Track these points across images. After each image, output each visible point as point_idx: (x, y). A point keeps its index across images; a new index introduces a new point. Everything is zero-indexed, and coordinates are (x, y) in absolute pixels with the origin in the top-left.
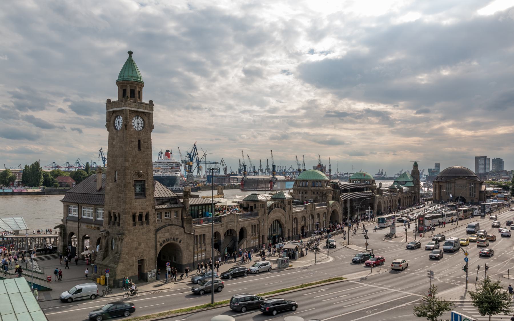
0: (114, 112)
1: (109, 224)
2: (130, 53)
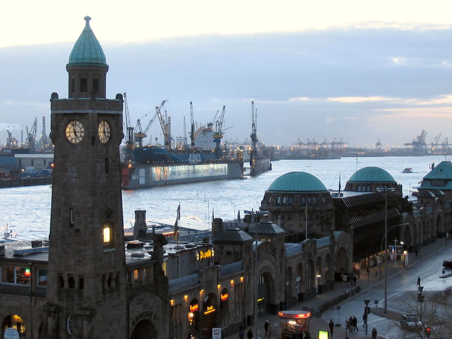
0: (65, 114)
1: (59, 292)
2: (88, 19)
